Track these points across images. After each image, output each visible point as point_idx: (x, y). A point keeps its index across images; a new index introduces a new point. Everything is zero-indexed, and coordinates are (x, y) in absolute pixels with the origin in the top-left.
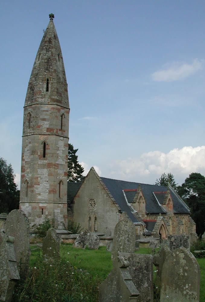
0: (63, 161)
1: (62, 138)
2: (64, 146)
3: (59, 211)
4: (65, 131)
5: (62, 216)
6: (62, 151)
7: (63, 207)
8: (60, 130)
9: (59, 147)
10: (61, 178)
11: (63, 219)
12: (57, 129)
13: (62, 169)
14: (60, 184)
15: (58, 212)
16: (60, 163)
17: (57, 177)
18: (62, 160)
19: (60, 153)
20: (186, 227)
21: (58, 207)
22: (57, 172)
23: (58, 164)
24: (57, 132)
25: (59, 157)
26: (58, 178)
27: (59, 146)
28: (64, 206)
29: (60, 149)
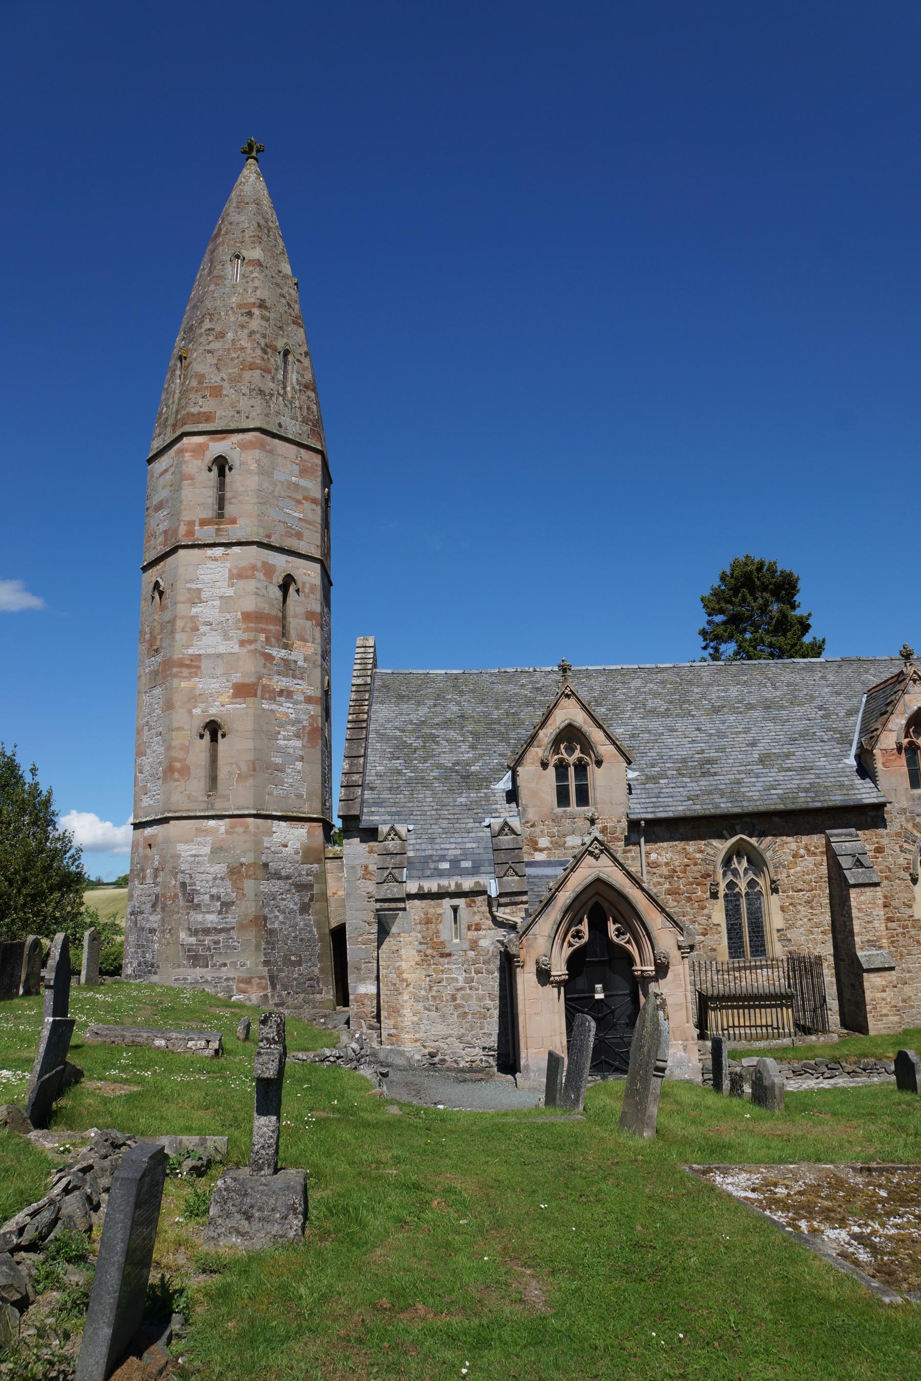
0: (226, 637)
1: (219, 551)
2: (232, 577)
3: (207, 850)
4: (233, 521)
5: (220, 869)
6: (217, 603)
7: (227, 832)
8: (203, 523)
9: (199, 591)
10: (213, 711)
11: (228, 883)
12: (191, 523)
13: (220, 671)
14: (214, 739)
15: (195, 856)
16: (211, 651)
17: (190, 712)
18: (219, 639)
19: (207, 611)
22: (192, 689)
23: (200, 655)
24: (190, 533)
25: (203, 629)
26: (197, 711)
27: (199, 586)
28: (231, 828)
29: (204, 595)
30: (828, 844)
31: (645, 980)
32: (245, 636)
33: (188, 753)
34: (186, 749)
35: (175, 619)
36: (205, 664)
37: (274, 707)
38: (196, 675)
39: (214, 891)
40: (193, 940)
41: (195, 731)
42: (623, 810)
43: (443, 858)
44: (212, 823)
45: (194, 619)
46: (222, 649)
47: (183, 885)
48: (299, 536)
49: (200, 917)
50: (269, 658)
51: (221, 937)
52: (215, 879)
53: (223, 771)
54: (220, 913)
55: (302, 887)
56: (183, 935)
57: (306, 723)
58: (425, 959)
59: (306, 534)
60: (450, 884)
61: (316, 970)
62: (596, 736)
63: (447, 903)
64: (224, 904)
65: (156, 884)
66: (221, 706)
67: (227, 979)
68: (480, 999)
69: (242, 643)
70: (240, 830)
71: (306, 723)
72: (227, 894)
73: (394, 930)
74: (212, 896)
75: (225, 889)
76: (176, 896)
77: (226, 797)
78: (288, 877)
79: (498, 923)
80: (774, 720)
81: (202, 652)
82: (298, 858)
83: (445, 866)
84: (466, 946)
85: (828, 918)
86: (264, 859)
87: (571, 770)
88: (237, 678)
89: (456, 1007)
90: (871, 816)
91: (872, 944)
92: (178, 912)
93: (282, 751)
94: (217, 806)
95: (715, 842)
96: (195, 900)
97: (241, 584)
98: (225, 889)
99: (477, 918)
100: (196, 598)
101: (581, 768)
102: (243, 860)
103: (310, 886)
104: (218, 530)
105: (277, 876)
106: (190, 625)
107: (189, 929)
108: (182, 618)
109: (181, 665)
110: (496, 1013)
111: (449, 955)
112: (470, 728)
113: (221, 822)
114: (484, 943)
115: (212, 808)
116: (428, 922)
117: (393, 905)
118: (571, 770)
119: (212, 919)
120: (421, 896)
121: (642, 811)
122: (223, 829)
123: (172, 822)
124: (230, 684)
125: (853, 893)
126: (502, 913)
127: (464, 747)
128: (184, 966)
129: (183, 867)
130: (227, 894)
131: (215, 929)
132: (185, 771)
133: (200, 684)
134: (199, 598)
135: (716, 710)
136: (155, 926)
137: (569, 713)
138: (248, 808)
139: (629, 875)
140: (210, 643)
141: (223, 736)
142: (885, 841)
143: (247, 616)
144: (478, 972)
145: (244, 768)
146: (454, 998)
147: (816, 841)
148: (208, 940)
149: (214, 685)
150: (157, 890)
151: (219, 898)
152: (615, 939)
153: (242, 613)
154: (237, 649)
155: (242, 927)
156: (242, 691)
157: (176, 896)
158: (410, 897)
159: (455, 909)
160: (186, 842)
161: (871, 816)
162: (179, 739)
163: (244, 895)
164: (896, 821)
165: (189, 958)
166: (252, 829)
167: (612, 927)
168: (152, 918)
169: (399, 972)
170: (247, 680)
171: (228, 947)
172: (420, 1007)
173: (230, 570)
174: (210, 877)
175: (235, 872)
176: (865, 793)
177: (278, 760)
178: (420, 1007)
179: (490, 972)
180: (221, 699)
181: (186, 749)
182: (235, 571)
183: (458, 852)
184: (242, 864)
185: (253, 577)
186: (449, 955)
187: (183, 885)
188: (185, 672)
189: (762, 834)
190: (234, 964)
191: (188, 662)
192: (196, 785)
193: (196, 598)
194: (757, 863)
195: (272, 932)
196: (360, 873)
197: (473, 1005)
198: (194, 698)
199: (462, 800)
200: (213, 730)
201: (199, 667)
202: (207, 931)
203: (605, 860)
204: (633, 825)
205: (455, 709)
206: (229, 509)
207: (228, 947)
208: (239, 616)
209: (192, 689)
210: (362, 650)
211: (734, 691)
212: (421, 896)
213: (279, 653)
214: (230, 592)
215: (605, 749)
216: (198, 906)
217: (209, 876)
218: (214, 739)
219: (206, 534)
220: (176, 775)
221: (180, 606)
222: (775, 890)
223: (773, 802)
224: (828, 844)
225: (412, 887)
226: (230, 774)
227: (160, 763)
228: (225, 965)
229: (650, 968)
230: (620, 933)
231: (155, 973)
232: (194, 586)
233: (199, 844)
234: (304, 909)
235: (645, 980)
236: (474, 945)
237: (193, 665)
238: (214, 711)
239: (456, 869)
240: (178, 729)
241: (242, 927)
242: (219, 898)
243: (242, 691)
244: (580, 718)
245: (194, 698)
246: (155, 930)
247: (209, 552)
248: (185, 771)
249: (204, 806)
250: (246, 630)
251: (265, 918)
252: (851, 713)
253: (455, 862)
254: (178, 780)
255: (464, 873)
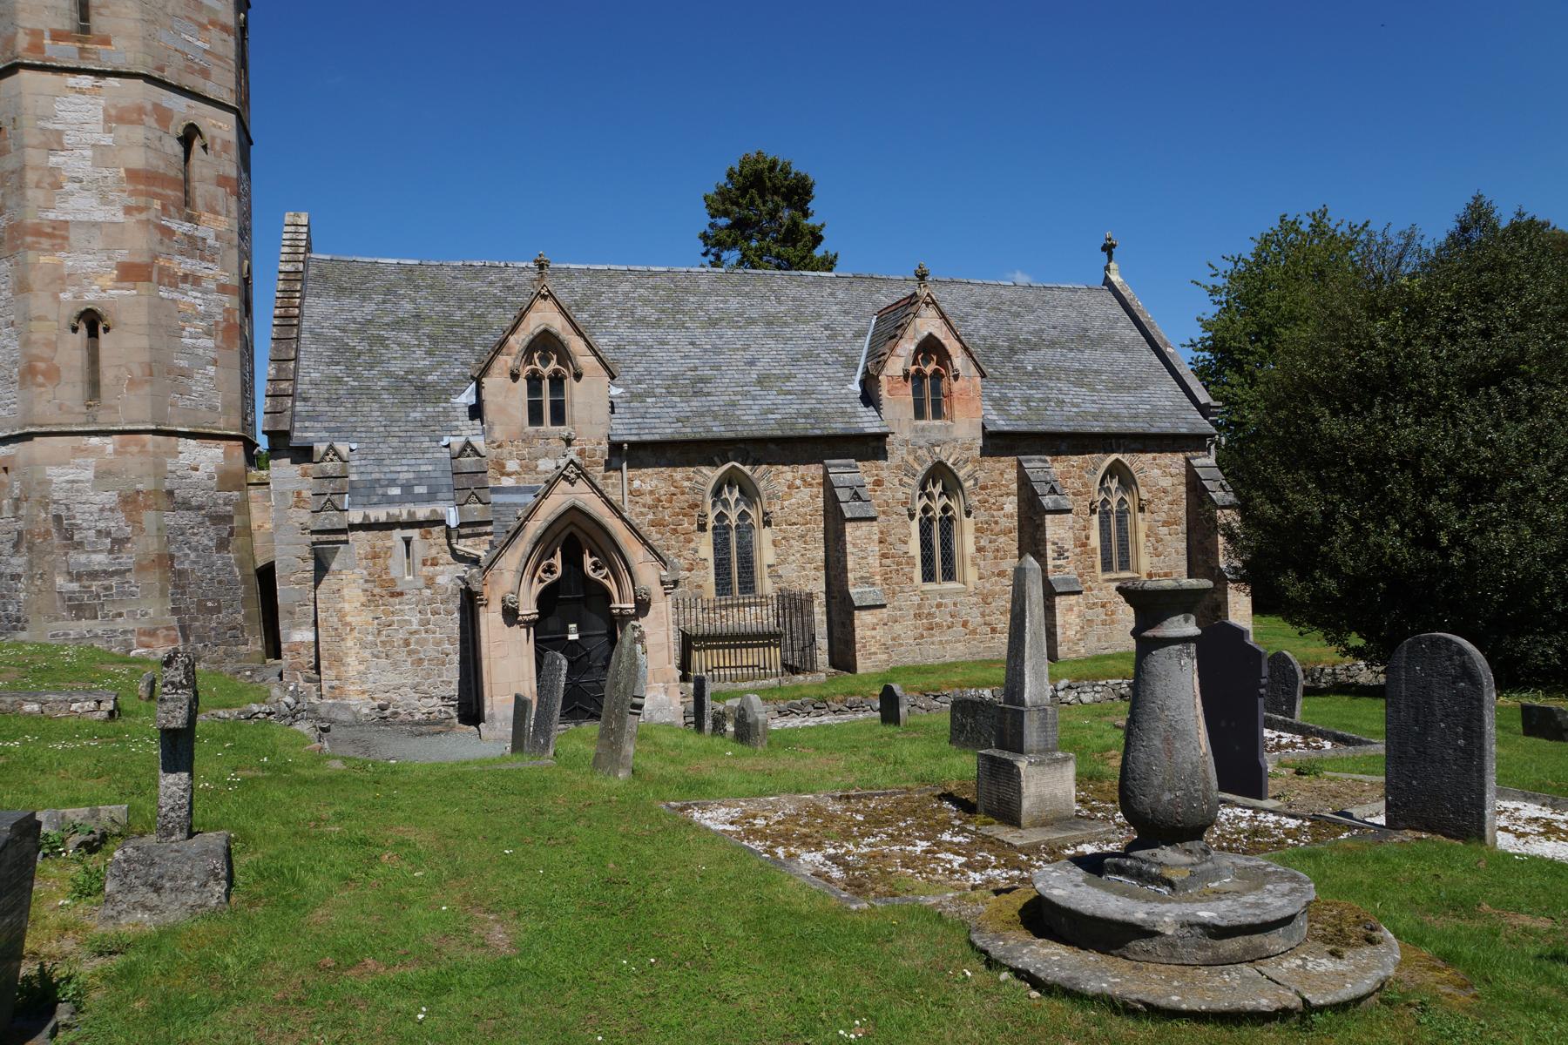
0: (104, 200)
1: (86, 81)
2: (108, 119)
3: (89, 474)
4: (106, 41)
5: (110, 498)
6: (88, 153)
9: (60, 133)
11: (120, 515)
13: (97, 244)
14: (93, 333)
16: (84, 218)
17: (56, 297)
19: (73, 163)
20: (1164, 530)
21: (77, 450)
25: (69, 186)
26: (66, 296)
29: (66, 140)
30: (826, 474)
31: (624, 618)
32: (132, 201)
33: (56, 350)
34: (52, 345)
35: (23, 168)
36: (74, 235)
37: (175, 295)
38: (62, 248)
39: (101, 525)
40: (75, 586)
41: (64, 322)
42: (602, 431)
43: (392, 483)
44: (94, 440)
45: (54, 171)
46: (98, 216)
47: (58, 518)
48: (205, 73)
49: (83, 558)
50: (167, 232)
51: (114, 581)
52: (102, 510)
53: (107, 376)
54: (111, 552)
55: (218, 519)
56: (60, 581)
57: (219, 318)
58: (372, 600)
59: (215, 71)
60: (402, 512)
61: (240, 617)
62: (576, 344)
63: (398, 534)
64: (115, 541)
65: (17, 518)
66: (102, 292)
67: (124, 632)
68: (438, 644)
69: (128, 210)
70: (134, 449)
71: (219, 318)
72: (119, 529)
73: (334, 566)
74: (99, 532)
75: (117, 523)
76: (48, 532)
77: (114, 409)
78: (200, 508)
79: (459, 557)
80: (776, 337)
81: (69, 218)
82: (212, 483)
83: (396, 491)
84: (421, 583)
85: (821, 554)
86: (167, 485)
87: (546, 384)
88: (123, 255)
89: (410, 653)
90: (871, 446)
91: (865, 580)
92: (51, 553)
93: (189, 352)
94: (101, 418)
95: (705, 470)
96: (76, 538)
97: (123, 130)
98: (117, 523)
99: (433, 552)
100: (54, 142)
101: (557, 382)
102: (139, 486)
103: (228, 518)
104: (82, 50)
105: (186, 505)
106: (49, 180)
107: (69, 573)
108: (35, 168)
109: (38, 232)
110: (457, 658)
111: (401, 594)
112: (427, 330)
113: (107, 440)
114: (441, 580)
115: (95, 422)
116: (375, 556)
117: (333, 537)
118: (546, 384)
119: (100, 560)
120: (367, 526)
121: (626, 432)
122: (110, 448)
123: (37, 439)
124: (113, 263)
125: (849, 527)
126: (463, 546)
127: (419, 353)
128: (64, 619)
129: (56, 496)
130: (119, 529)
131: (105, 572)
132: (53, 374)
133: (70, 261)
134: (60, 143)
135: (713, 323)
136: (20, 570)
137: (545, 317)
138: (144, 422)
139: (608, 503)
140: (79, 206)
141: (106, 330)
142: (884, 474)
143: (133, 175)
144: (434, 613)
145: (138, 372)
146: (407, 643)
147: (814, 471)
148: (95, 586)
149: (90, 263)
150: (20, 525)
151: (108, 534)
152: (591, 574)
153: (127, 170)
154: (120, 217)
155: (141, 568)
156: (130, 273)
157: (48, 532)
158: (353, 527)
159: (408, 541)
160: (59, 465)
161: (871, 446)
162: (40, 332)
163: (142, 530)
164: (897, 452)
165: (70, 608)
166: (150, 447)
167: (588, 561)
168: (13, 561)
169: (341, 615)
170: (137, 260)
171: (124, 593)
172: (367, 654)
173: (105, 110)
174: (95, 508)
175: (130, 502)
176: (868, 422)
177: (183, 363)
178: (367, 654)
179: (449, 613)
180: (101, 281)
181: (52, 345)
182: (113, 112)
183: (411, 476)
184: (138, 492)
185: (140, 122)
186: (401, 594)
187: (58, 518)
188: (46, 243)
189: (756, 462)
190: (133, 613)
191: (49, 230)
192: (71, 392)
193: (54, 142)
194: (749, 493)
195: (181, 574)
196: (292, 500)
197: (430, 651)
198: (61, 279)
199: (417, 415)
200: (92, 321)
201: (66, 238)
202: (94, 575)
203: (581, 485)
204: (615, 447)
205: (409, 306)
206: (98, 23)
207: (124, 593)
208: (122, 173)
209: (58, 267)
210: (292, 229)
211: (734, 303)
212: (367, 526)
213: (180, 227)
214: (107, 140)
215: (586, 361)
216: (80, 544)
217: (93, 506)
218: (93, 333)
219: (65, 53)
220: (40, 379)
221: (29, 151)
222: (767, 523)
223: (770, 428)
224: (826, 474)
225: (356, 516)
226: (118, 379)
227: (15, 362)
228: (120, 615)
229: (630, 606)
230: (596, 567)
231: (23, 629)
232: (50, 126)
233: (78, 466)
234: (222, 545)
235: (624, 618)
236: (430, 582)
237: (58, 234)
238: (91, 297)
239: (408, 495)
240: (39, 318)
241: (141, 568)
242: (108, 534)
243: (130, 273)
244: (558, 324)
245: (61, 278)
246: (19, 576)
247: (72, 80)
248: (53, 374)
249: (83, 419)
250: (133, 193)
251: (172, 557)
252: (859, 335)
253: (407, 487)
254: (42, 385)
255: (419, 499)
